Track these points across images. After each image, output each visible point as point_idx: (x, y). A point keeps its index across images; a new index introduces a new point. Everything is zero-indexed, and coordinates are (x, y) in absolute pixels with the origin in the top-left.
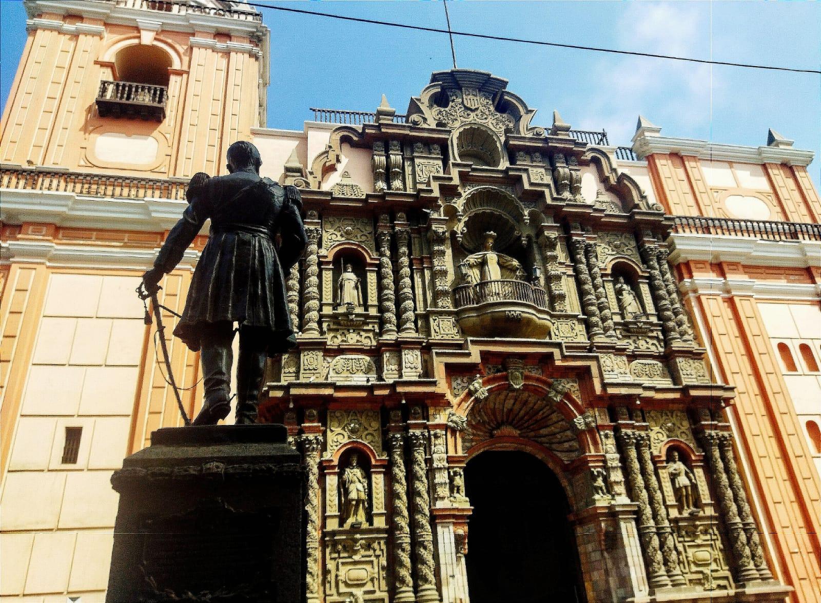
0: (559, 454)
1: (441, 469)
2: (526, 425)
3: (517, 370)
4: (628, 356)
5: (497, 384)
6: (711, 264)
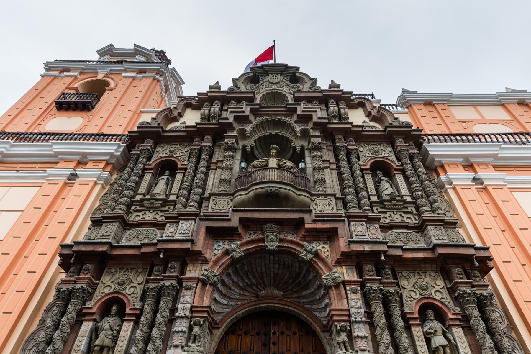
0: (318, 315)
1: (182, 317)
2: (290, 288)
3: (272, 233)
4: (381, 227)
5: (253, 246)
6: (464, 167)
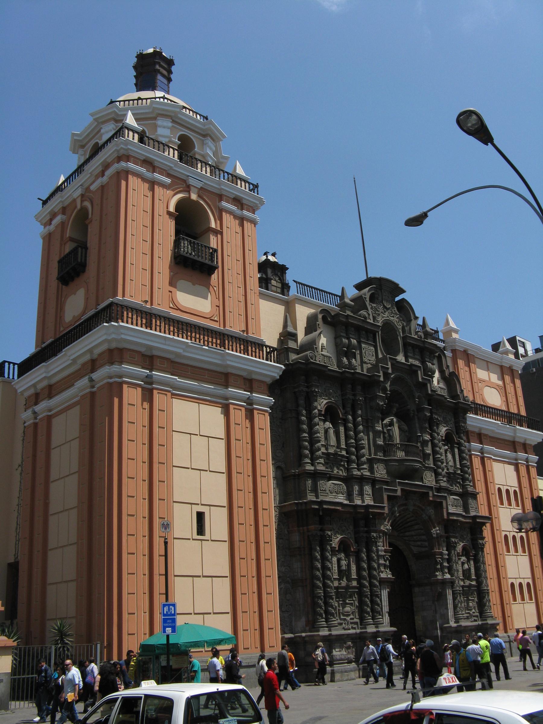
0: (413, 548)
